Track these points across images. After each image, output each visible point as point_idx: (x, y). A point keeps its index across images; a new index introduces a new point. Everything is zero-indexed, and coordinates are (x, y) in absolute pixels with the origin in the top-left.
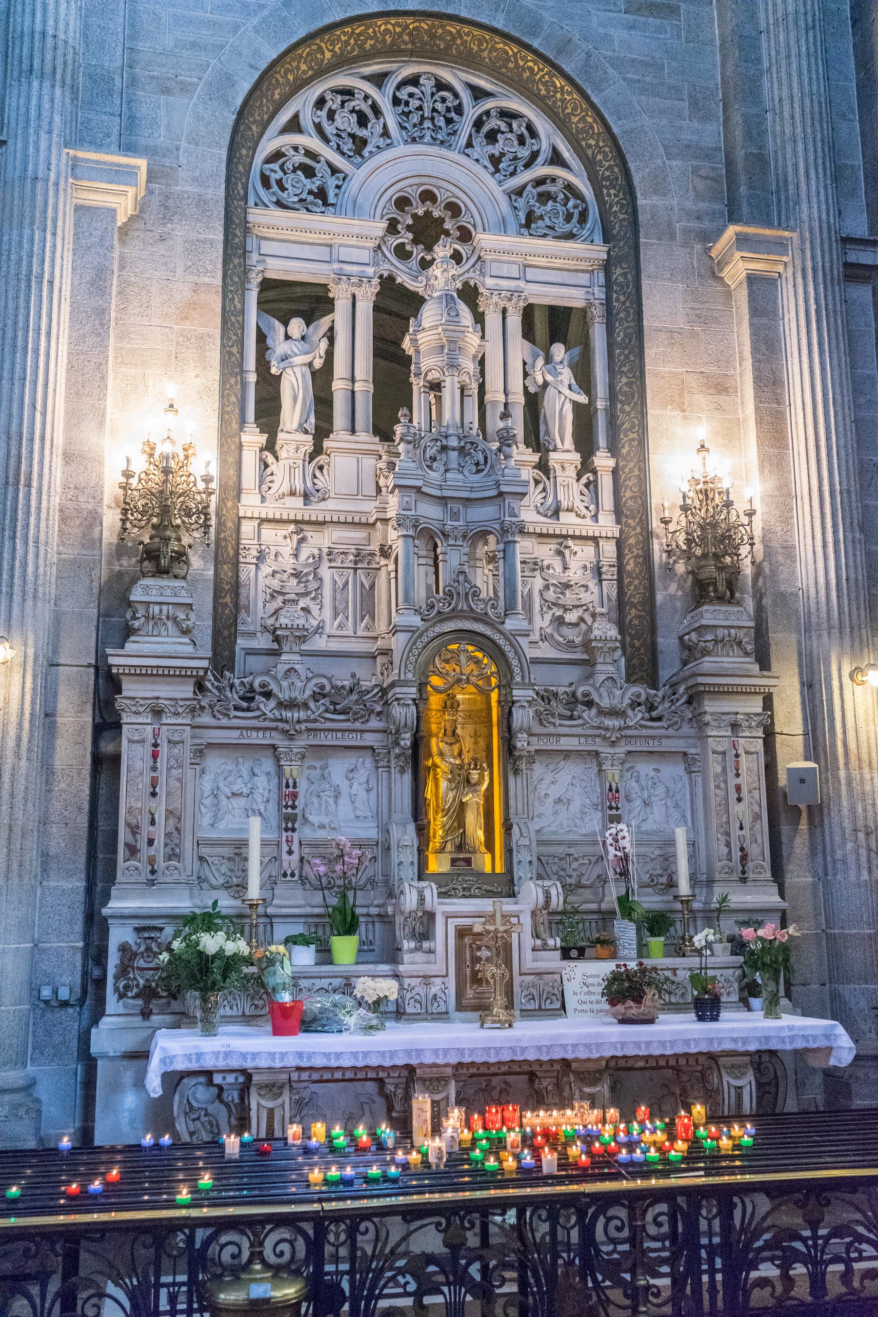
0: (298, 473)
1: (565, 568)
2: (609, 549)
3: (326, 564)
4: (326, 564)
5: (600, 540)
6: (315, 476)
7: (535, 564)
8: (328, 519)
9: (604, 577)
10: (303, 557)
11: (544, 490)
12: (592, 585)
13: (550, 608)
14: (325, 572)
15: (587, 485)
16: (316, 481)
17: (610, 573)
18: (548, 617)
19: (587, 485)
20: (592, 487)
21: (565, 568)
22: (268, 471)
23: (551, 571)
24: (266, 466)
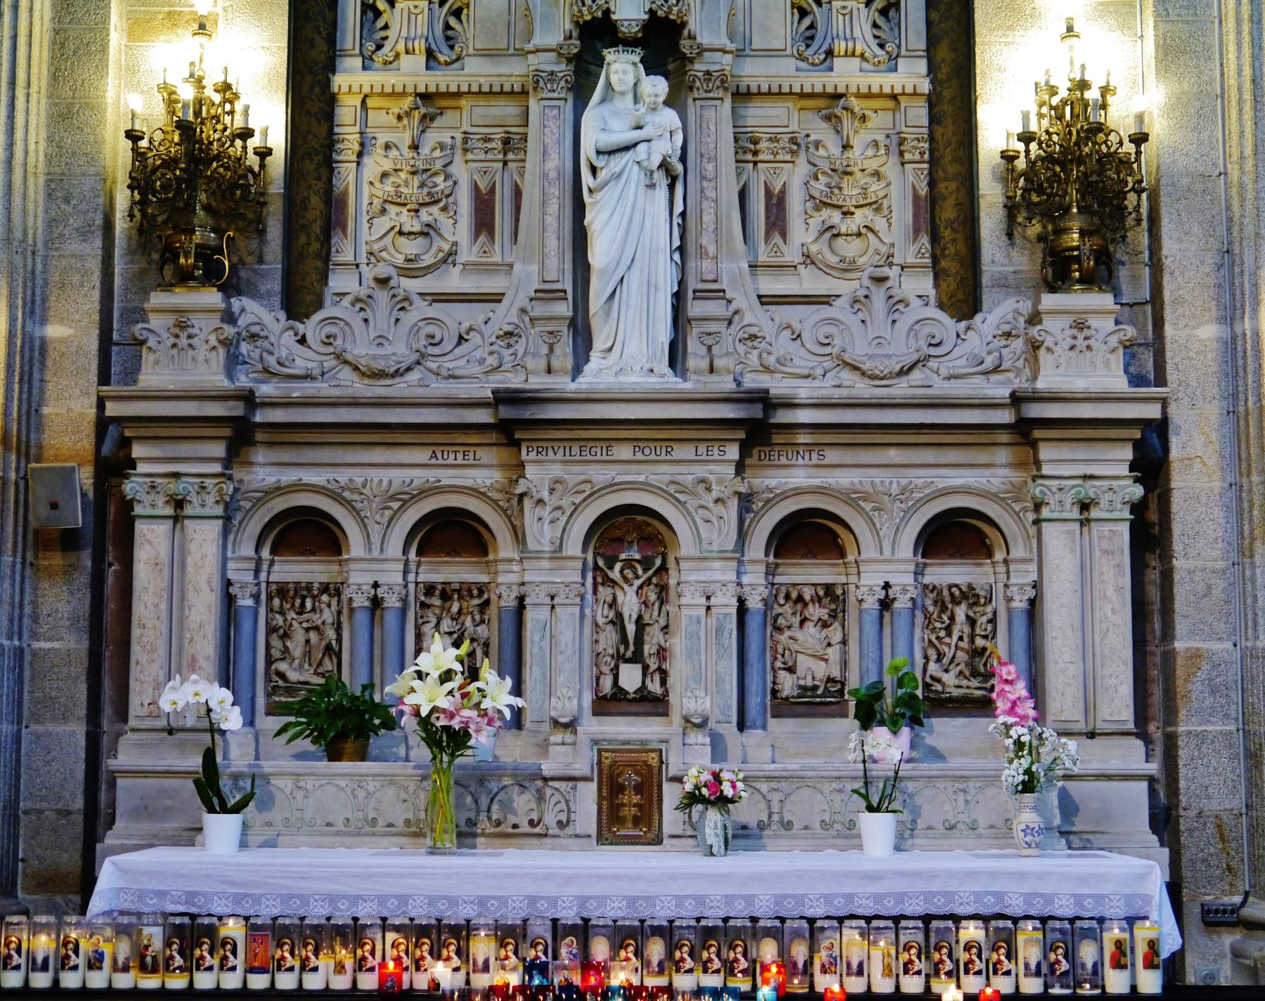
0: (422, 20)
1: (846, 147)
2: (919, 114)
3: (458, 158)
4: (458, 158)
5: (901, 99)
6: (447, 27)
7: (793, 141)
8: (464, 89)
9: (908, 156)
10: (425, 150)
11: (812, 26)
12: (891, 168)
13: (817, 209)
14: (460, 170)
15: (884, 12)
16: (450, 33)
17: (917, 149)
18: (816, 221)
19: (884, 12)
20: (892, 13)
21: (846, 147)
22: (380, 23)
23: (822, 152)
24: (378, 14)
